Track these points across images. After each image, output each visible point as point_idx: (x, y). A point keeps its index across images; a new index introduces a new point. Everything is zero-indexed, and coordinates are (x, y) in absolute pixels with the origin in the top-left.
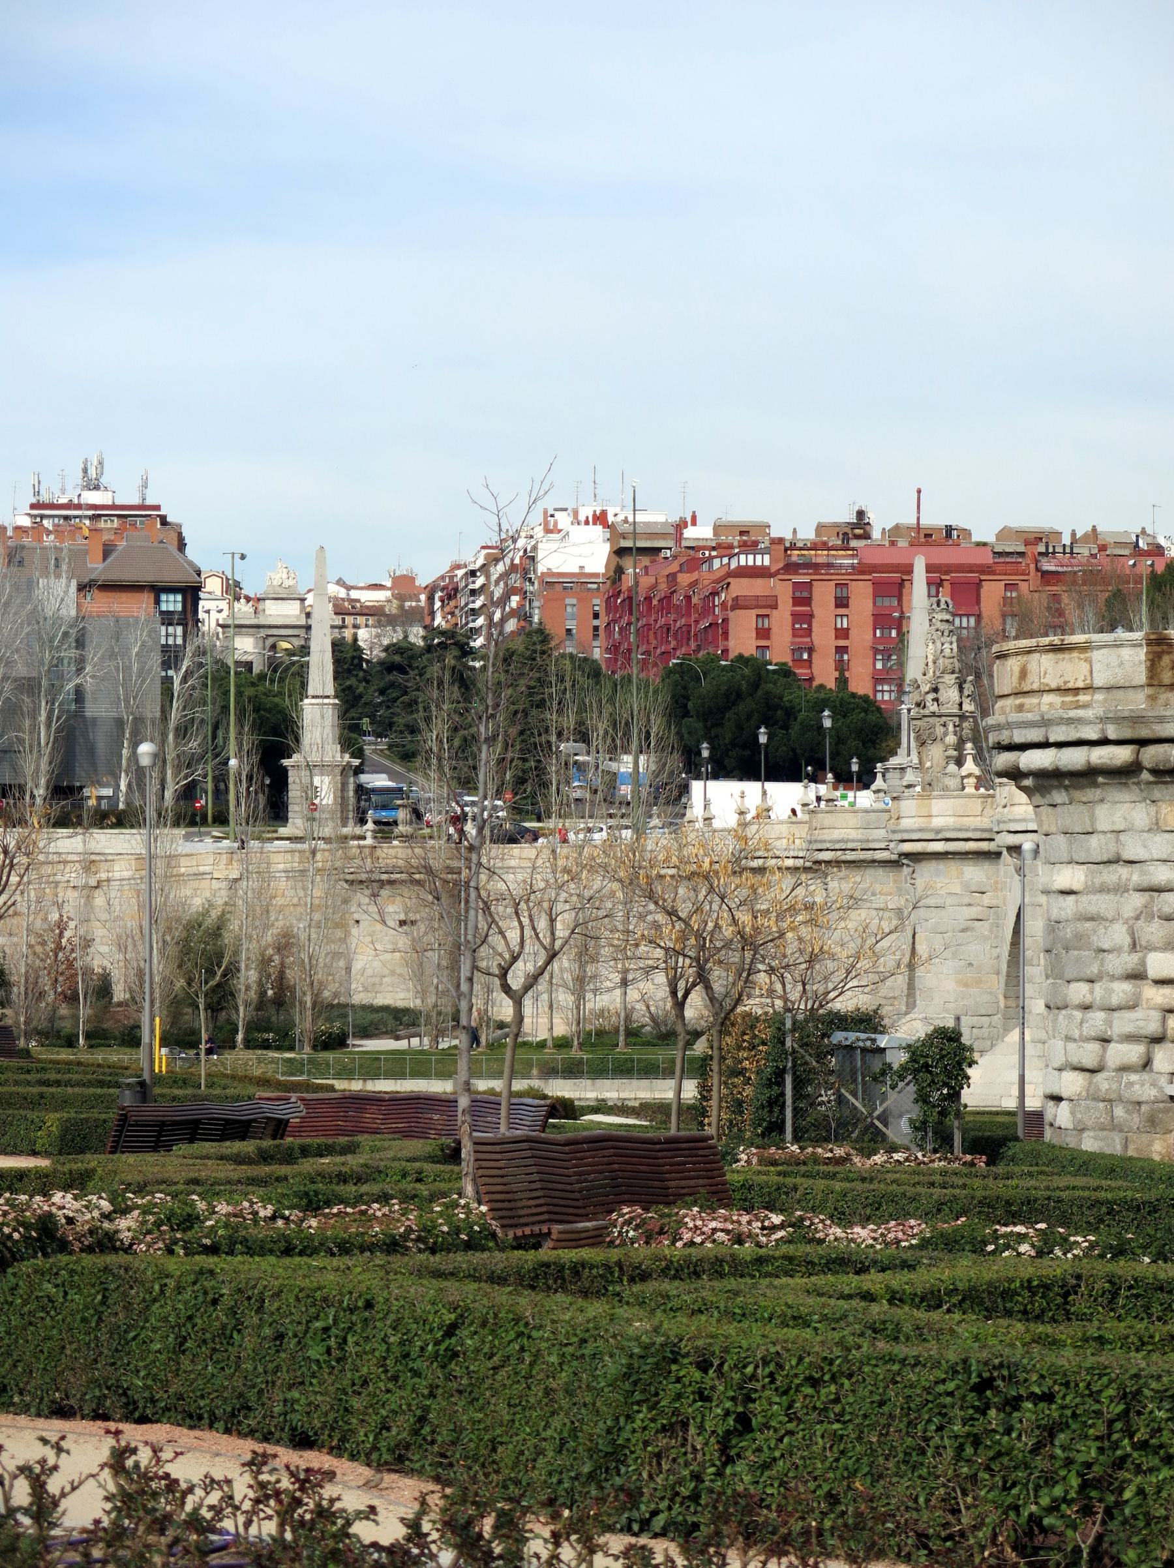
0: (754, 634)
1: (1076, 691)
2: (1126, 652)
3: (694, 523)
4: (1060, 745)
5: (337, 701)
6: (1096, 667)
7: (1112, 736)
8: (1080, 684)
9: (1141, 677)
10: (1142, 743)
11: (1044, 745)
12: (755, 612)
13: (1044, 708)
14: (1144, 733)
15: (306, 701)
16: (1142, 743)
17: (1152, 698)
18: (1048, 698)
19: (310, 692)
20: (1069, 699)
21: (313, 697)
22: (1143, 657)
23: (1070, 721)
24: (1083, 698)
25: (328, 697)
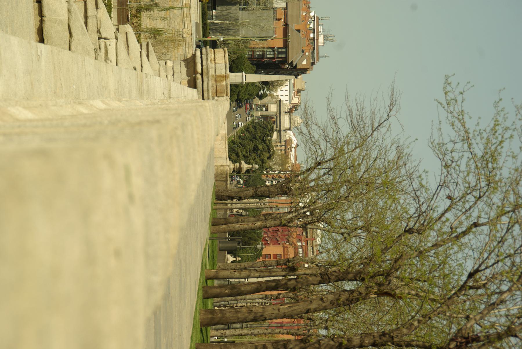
0: (275, 253)
1: (215, 61)
2: (224, 70)
3: (281, 91)
4: (201, 58)
5: (244, 83)
6: (221, 65)
7: (203, 67)
8: (216, 61)
9: (217, 74)
10: (202, 74)
11: (201, 54)
12: (282, 254)
13: (211, 55)
14: (204, 74)
15: (244, 73)
16: (202, 74)
17: (213, 76)
18: (213, 56)
19: (248, 75)
20: (213, 60)
21: (245, 76)
22: (223, 74)
23: (207, 59)
24: (213, 62)
25: (245, 80)
